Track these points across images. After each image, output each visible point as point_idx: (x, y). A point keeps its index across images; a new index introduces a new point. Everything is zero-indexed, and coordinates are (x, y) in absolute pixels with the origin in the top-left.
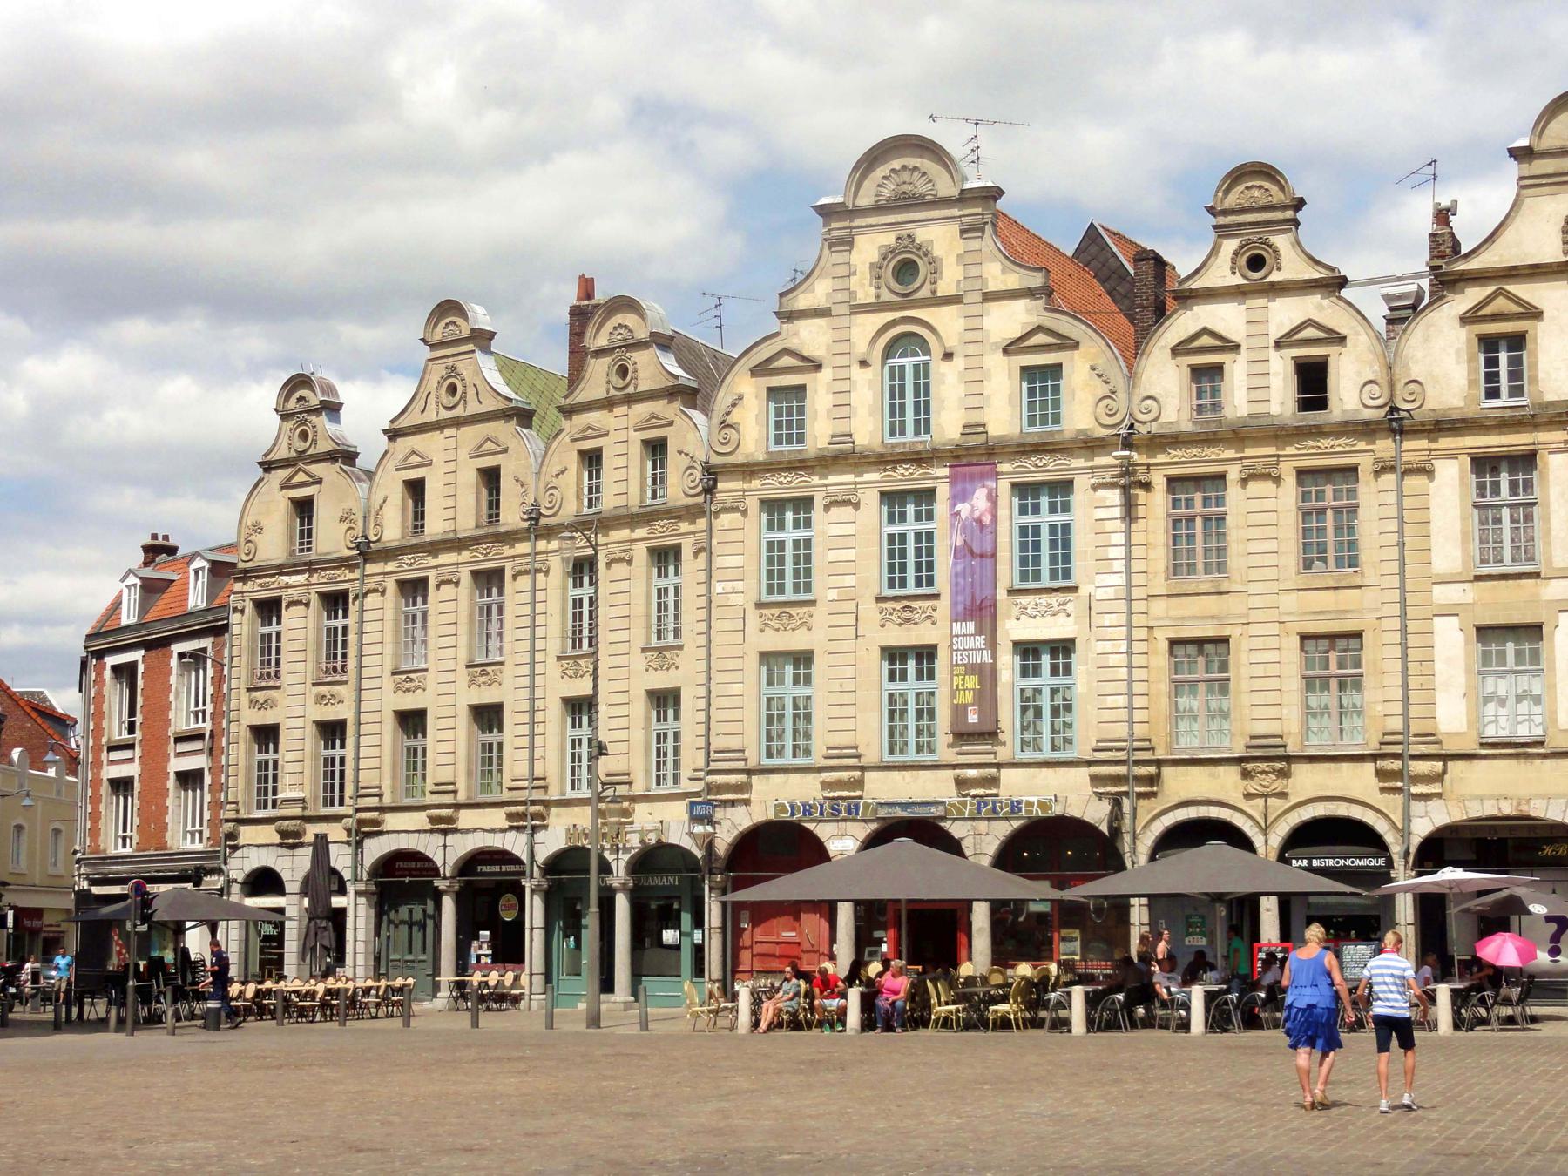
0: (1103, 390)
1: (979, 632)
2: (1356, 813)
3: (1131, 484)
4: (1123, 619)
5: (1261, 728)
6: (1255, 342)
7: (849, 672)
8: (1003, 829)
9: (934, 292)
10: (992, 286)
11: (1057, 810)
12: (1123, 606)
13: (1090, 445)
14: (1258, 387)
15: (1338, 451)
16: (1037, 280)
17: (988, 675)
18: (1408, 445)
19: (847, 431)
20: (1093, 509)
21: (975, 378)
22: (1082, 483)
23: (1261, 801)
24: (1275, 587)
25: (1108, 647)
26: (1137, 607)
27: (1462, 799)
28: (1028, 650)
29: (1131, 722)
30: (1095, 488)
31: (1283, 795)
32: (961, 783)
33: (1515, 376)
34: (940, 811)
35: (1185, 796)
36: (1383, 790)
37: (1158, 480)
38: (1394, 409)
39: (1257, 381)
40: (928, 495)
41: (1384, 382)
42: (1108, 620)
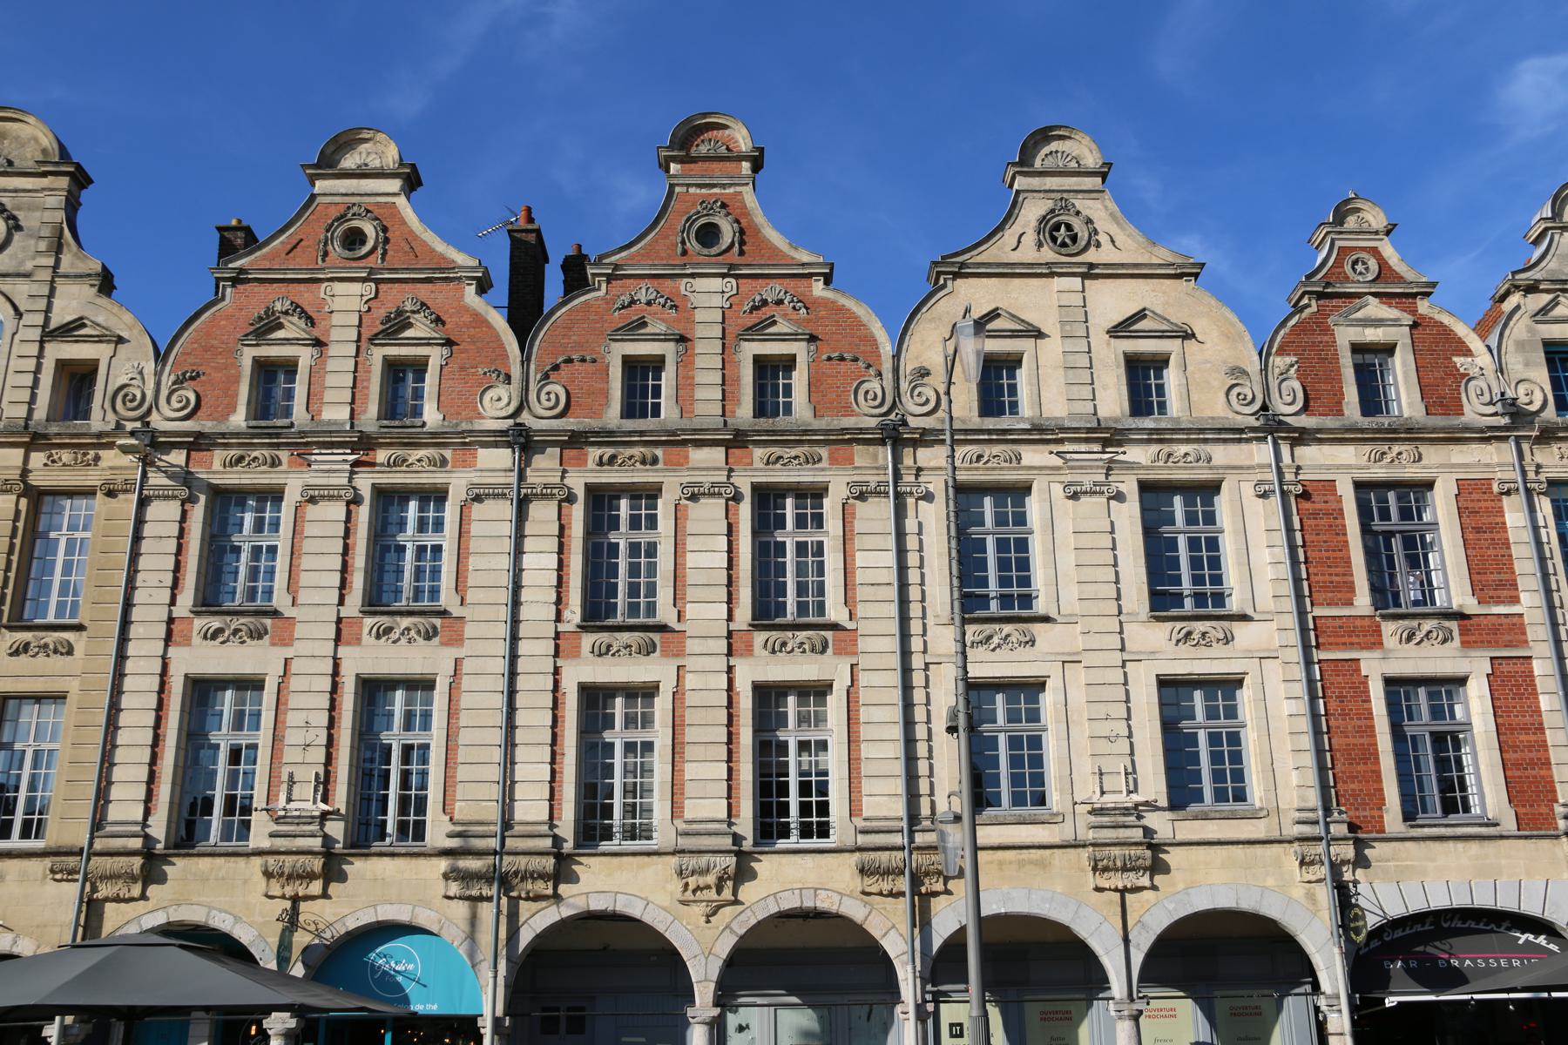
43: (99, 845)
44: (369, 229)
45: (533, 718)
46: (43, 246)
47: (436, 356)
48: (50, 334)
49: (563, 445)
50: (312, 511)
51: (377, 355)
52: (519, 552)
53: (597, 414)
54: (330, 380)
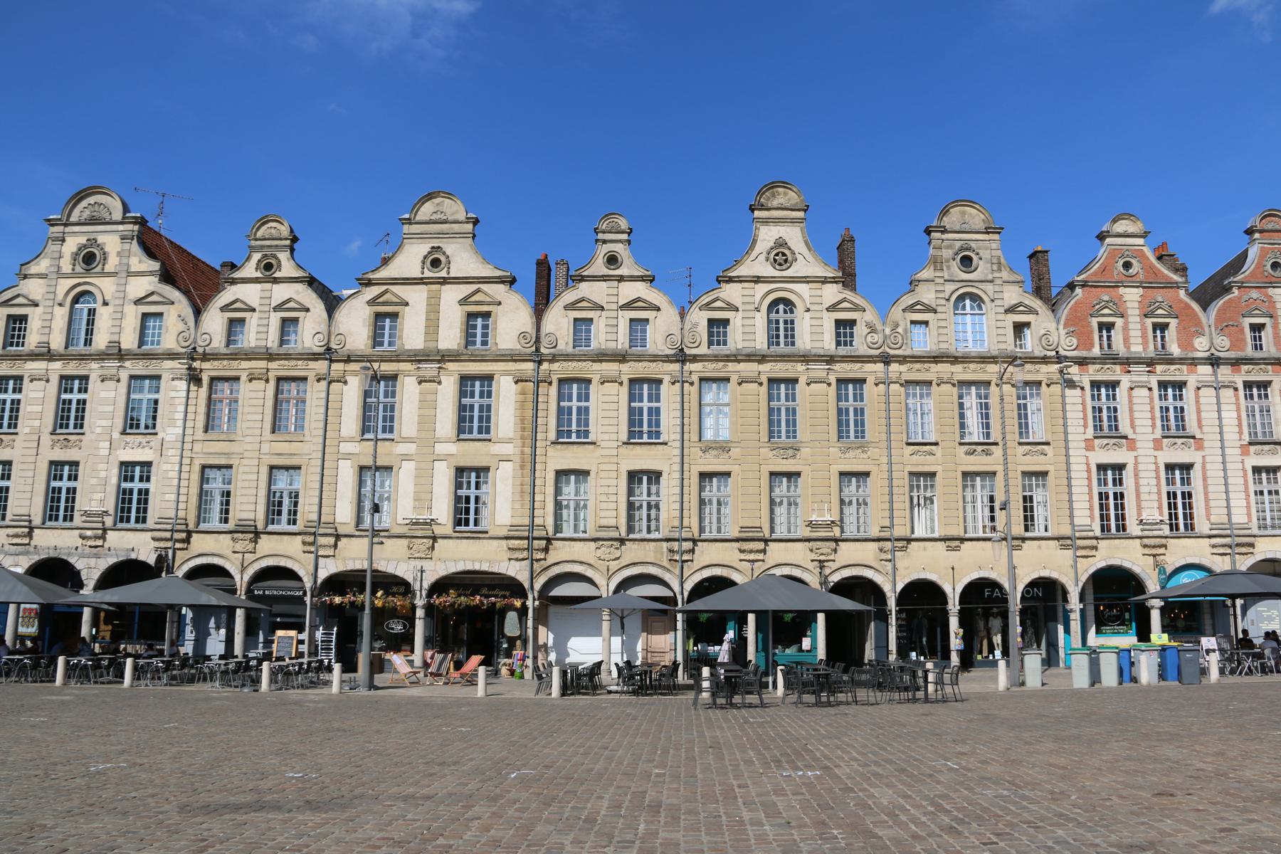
0: (181, 327)
13: (172, 356)
15: (298, 368)
18: (335, 366)
22: (166, 377)
27: (344, 559)
35: (200, 551)
38: (329, 349)
41: (326, 334)
42: (171, 452)
43: (1077, 534)
44: (1134, 261)
45: (1236, 481)
46: (995, 267)
47: (1173, 323)
48: (1008, 311)
49: (1233, 365)
50: (1136, 392)
51: (1149, 322)
52: (1219, 411)
53: (1242, 350)
54: (1132, 333)
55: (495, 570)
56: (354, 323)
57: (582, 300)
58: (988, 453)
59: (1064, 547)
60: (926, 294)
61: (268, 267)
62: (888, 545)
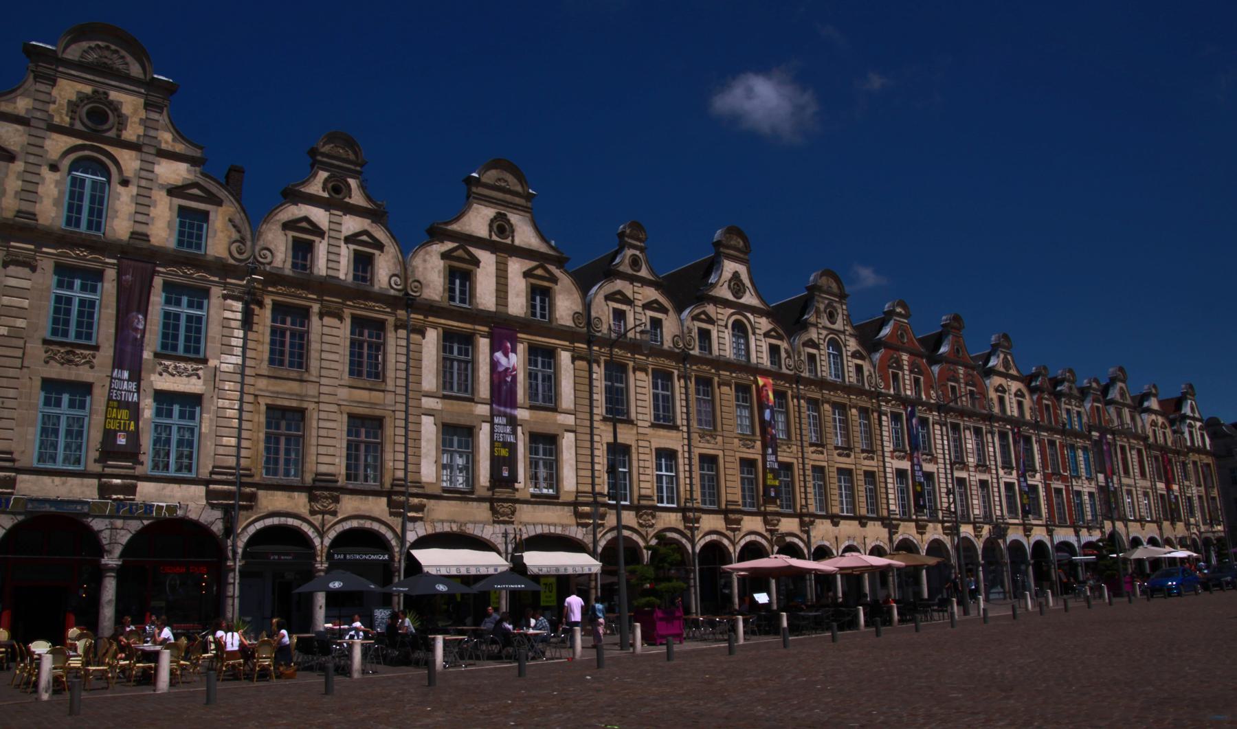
1: (130, 379)
2: (376, 526)
3: (251, 301)
4: (238, 387)
5: (323, 469)
6: (333, 234)
7: (12, 393)
8: (135, 525)
9: (119, 136)
10: (164, 146)
11: (180, 513)
12: (238, 378)
14: (332, 260)
16: (197, 153)
17: (135, 410)
19: (31, 210)
20: (223, 312)
21: (143, 202)
22: (216, 291)
23: (320, 517)
24: (337, 382)
25: (227, 403)
26: (248, 380)
27: (433, 522)
28: (164, 399)
29: (238, 457)
30: (225, 297)
31: (334, 513)
32: (104, 490)
33: (463, 292)
34: (86, 509)
35: (271, 509)
36: (391, 514)
37: (268, 301)
39: (332, 257)
40: (99, 275)
42: (227, 386)
55: (567, 533)
56: (431, 270)
57: (620, 292)
58: (848, 456)
59: (884, 526)
60: (813, 334)
61: (336, 190)
62: (807, 519)
